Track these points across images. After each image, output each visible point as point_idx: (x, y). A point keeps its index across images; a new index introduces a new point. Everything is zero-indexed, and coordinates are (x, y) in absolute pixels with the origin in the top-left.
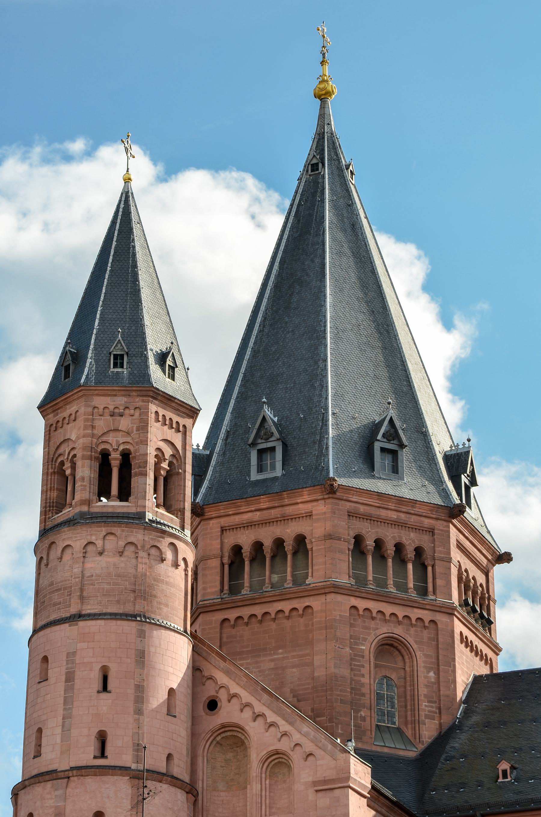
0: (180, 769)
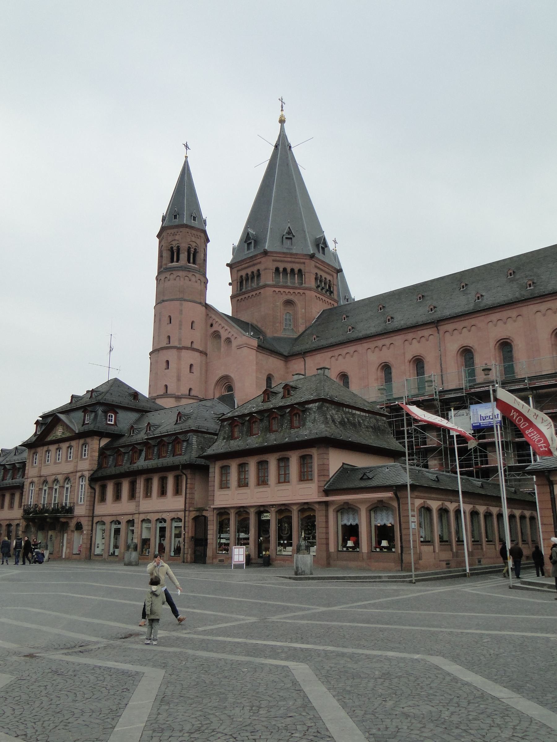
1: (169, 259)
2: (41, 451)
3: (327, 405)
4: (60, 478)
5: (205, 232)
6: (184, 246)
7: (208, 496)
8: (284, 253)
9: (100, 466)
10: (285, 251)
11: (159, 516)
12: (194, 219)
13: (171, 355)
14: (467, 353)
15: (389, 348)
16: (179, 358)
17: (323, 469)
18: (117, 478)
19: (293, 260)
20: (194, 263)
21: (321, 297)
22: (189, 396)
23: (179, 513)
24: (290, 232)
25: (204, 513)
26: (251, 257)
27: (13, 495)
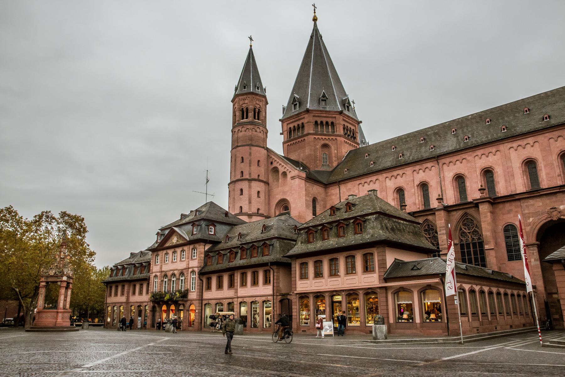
1: (241, 117)
2: (162, 254)
3: (382, 216)
4: (176, 272)
5: (265, 97)
6: (251, 107)
7: (291, 284)
8: (321, 111)
9: (206, 264)
10: (321, 109)
12: (258, 89)
13: (244, 185)
14: (460, 179)
15: (402, 177)
16: (250, 187)
17: (383, 263)
18: (219, 272)
19: (327, 115)
20: (258, 119)
21: (348, 141)
22: (258, 214)
23: (269, 297)
24: (324, 96)
25: (289, 297)
26: (297, 114)
27: (141, 285)
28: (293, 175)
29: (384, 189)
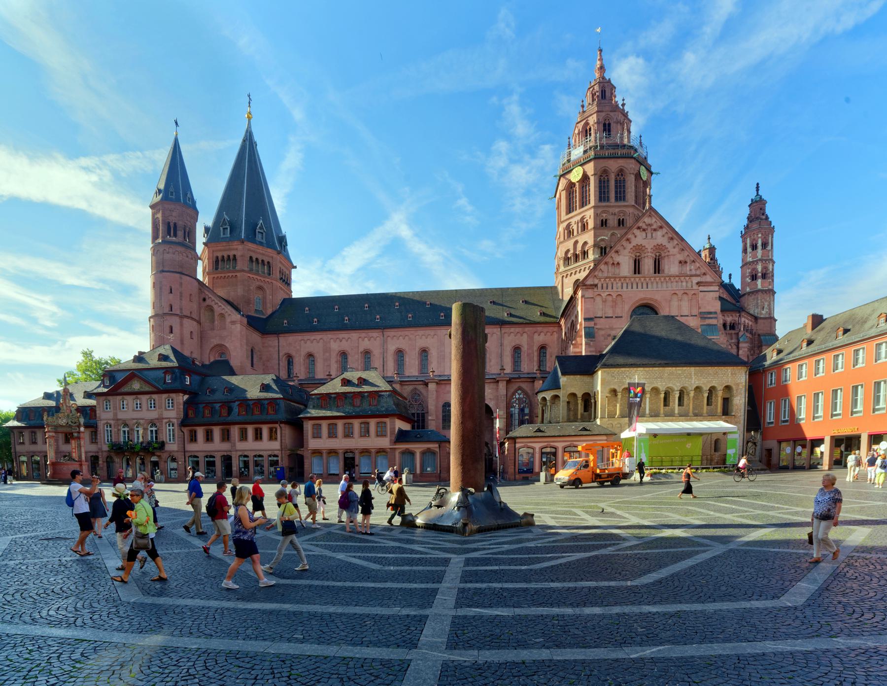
0: (195, 316)
11: (258, 453)
13: (175, 322)
16: (181, 325)
17: (393, 429)
28: (234, 319)
29: (327, 350)
